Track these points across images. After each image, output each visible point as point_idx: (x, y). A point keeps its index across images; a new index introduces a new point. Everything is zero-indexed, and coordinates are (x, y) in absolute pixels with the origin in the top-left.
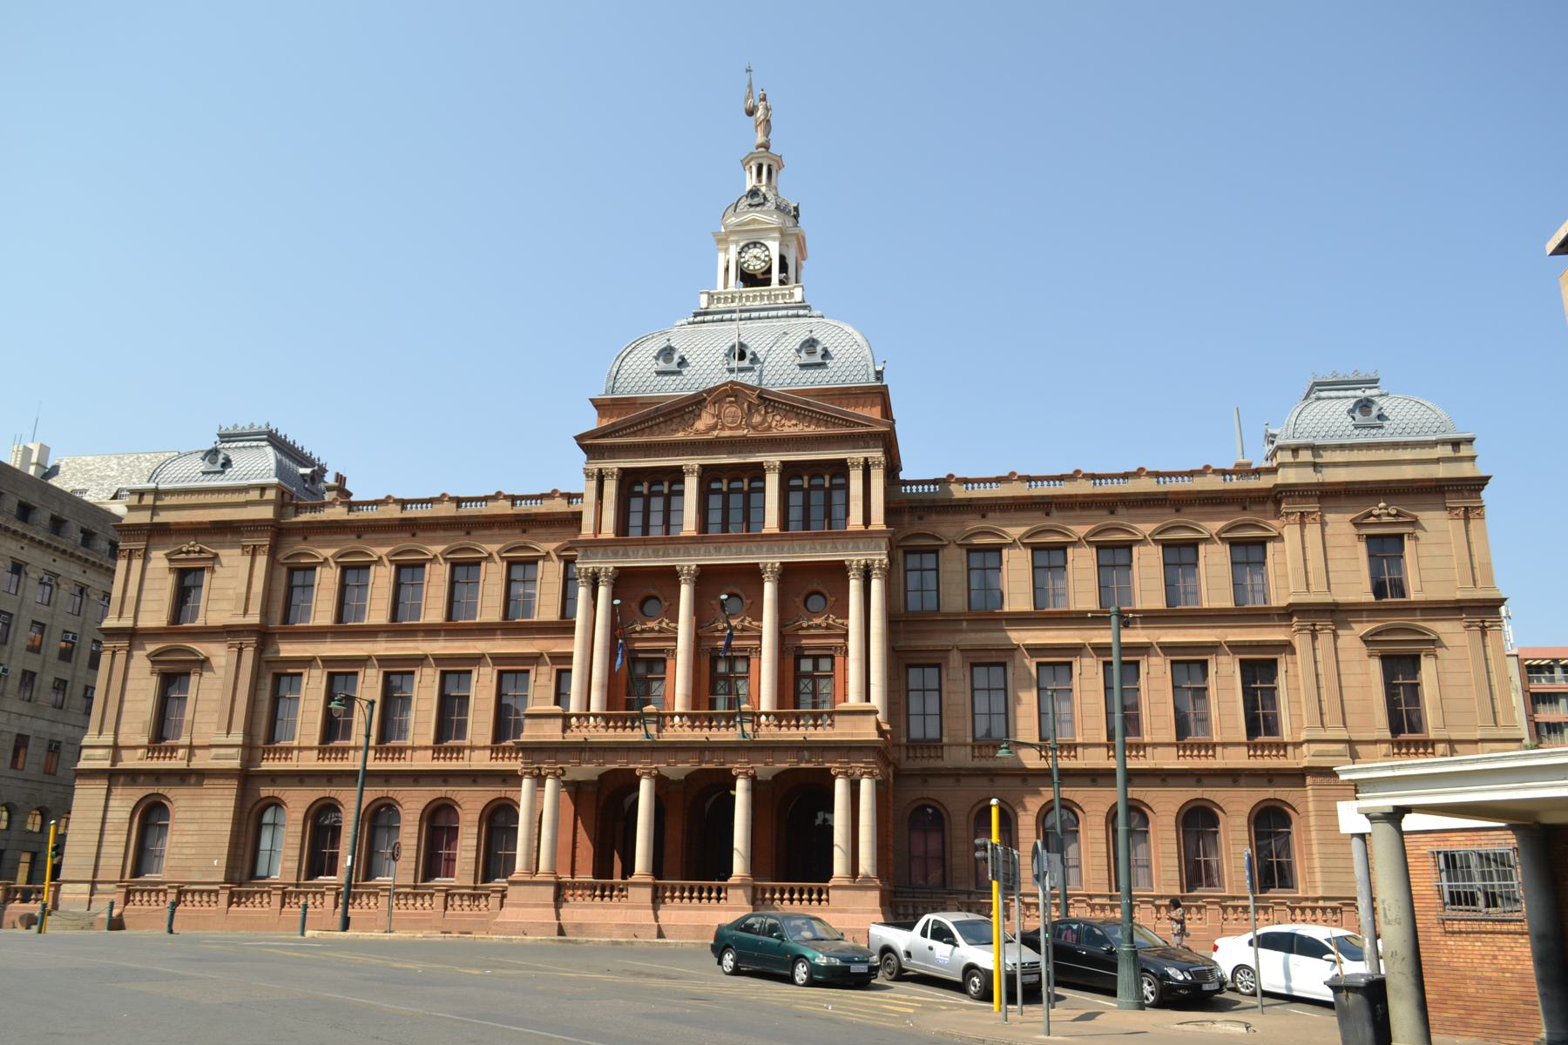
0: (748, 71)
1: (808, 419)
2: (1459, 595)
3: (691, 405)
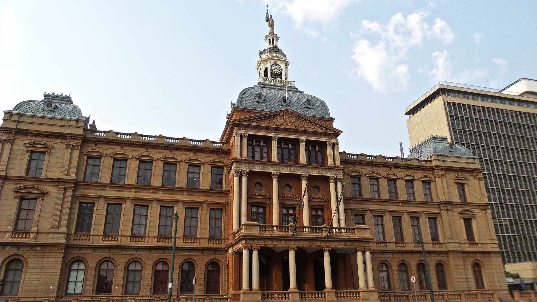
0: (267, 7)
2: (480, 202)
3: (274, 115)
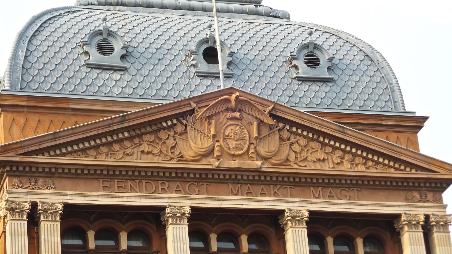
1: (339, 153)
3: (170, 118)
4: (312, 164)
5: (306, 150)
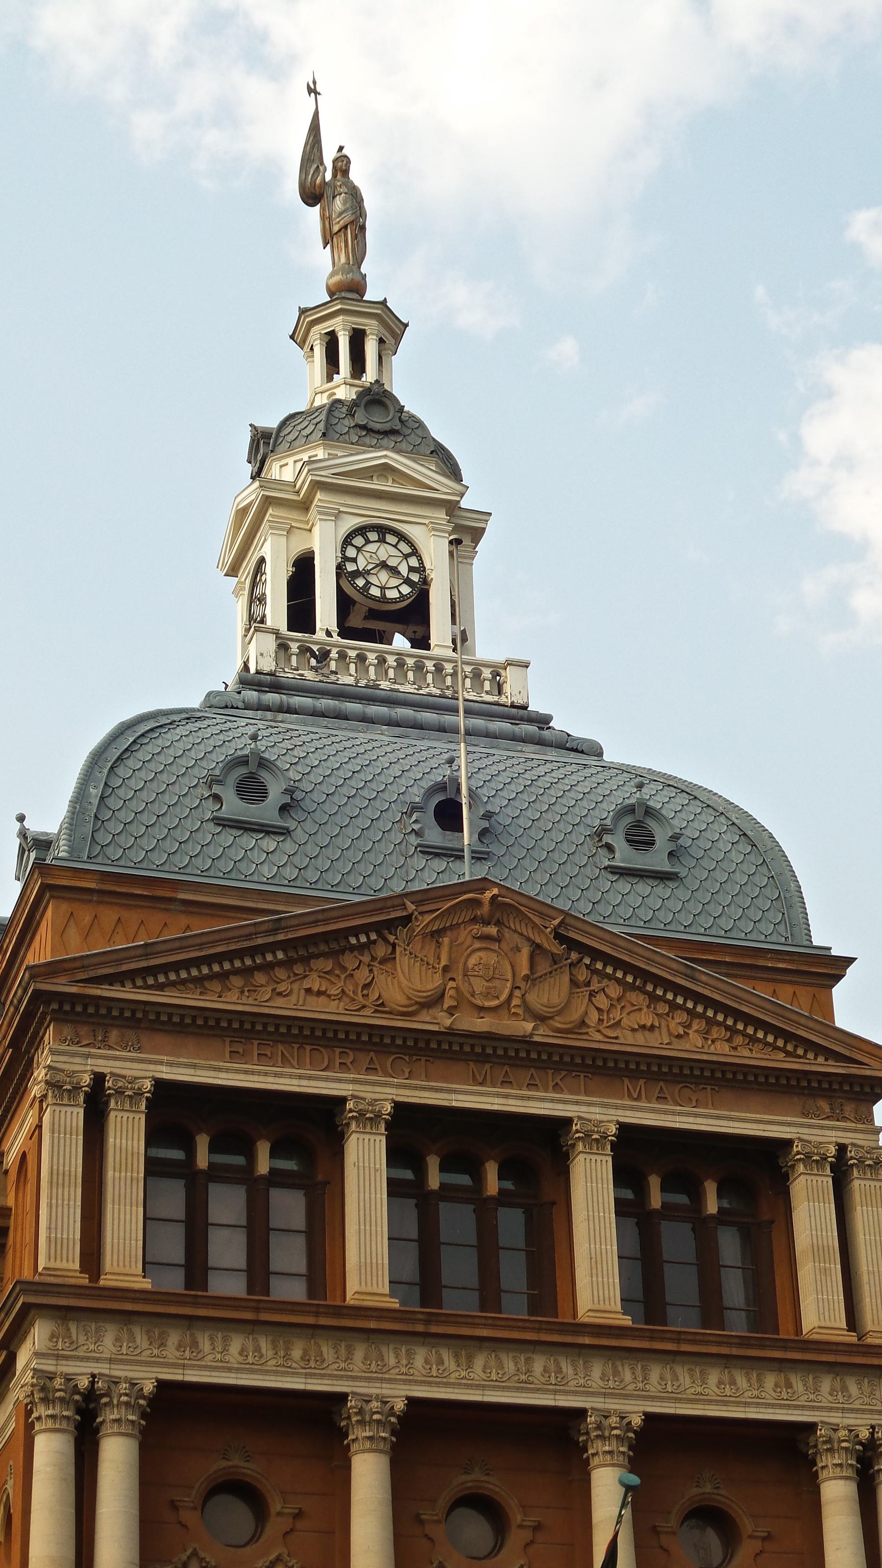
0: (312, 90)
1: (681, 1017)
3: (365, 929)
4: (629, 1034)
5: (619, 1007)
